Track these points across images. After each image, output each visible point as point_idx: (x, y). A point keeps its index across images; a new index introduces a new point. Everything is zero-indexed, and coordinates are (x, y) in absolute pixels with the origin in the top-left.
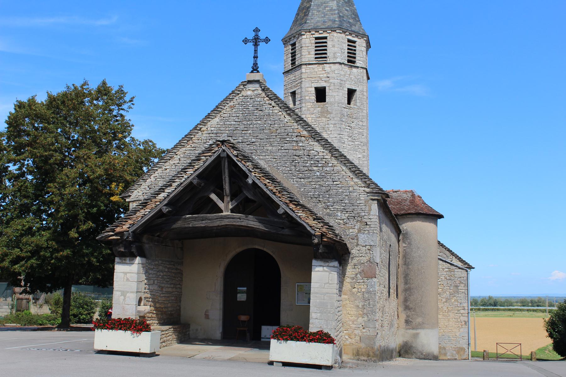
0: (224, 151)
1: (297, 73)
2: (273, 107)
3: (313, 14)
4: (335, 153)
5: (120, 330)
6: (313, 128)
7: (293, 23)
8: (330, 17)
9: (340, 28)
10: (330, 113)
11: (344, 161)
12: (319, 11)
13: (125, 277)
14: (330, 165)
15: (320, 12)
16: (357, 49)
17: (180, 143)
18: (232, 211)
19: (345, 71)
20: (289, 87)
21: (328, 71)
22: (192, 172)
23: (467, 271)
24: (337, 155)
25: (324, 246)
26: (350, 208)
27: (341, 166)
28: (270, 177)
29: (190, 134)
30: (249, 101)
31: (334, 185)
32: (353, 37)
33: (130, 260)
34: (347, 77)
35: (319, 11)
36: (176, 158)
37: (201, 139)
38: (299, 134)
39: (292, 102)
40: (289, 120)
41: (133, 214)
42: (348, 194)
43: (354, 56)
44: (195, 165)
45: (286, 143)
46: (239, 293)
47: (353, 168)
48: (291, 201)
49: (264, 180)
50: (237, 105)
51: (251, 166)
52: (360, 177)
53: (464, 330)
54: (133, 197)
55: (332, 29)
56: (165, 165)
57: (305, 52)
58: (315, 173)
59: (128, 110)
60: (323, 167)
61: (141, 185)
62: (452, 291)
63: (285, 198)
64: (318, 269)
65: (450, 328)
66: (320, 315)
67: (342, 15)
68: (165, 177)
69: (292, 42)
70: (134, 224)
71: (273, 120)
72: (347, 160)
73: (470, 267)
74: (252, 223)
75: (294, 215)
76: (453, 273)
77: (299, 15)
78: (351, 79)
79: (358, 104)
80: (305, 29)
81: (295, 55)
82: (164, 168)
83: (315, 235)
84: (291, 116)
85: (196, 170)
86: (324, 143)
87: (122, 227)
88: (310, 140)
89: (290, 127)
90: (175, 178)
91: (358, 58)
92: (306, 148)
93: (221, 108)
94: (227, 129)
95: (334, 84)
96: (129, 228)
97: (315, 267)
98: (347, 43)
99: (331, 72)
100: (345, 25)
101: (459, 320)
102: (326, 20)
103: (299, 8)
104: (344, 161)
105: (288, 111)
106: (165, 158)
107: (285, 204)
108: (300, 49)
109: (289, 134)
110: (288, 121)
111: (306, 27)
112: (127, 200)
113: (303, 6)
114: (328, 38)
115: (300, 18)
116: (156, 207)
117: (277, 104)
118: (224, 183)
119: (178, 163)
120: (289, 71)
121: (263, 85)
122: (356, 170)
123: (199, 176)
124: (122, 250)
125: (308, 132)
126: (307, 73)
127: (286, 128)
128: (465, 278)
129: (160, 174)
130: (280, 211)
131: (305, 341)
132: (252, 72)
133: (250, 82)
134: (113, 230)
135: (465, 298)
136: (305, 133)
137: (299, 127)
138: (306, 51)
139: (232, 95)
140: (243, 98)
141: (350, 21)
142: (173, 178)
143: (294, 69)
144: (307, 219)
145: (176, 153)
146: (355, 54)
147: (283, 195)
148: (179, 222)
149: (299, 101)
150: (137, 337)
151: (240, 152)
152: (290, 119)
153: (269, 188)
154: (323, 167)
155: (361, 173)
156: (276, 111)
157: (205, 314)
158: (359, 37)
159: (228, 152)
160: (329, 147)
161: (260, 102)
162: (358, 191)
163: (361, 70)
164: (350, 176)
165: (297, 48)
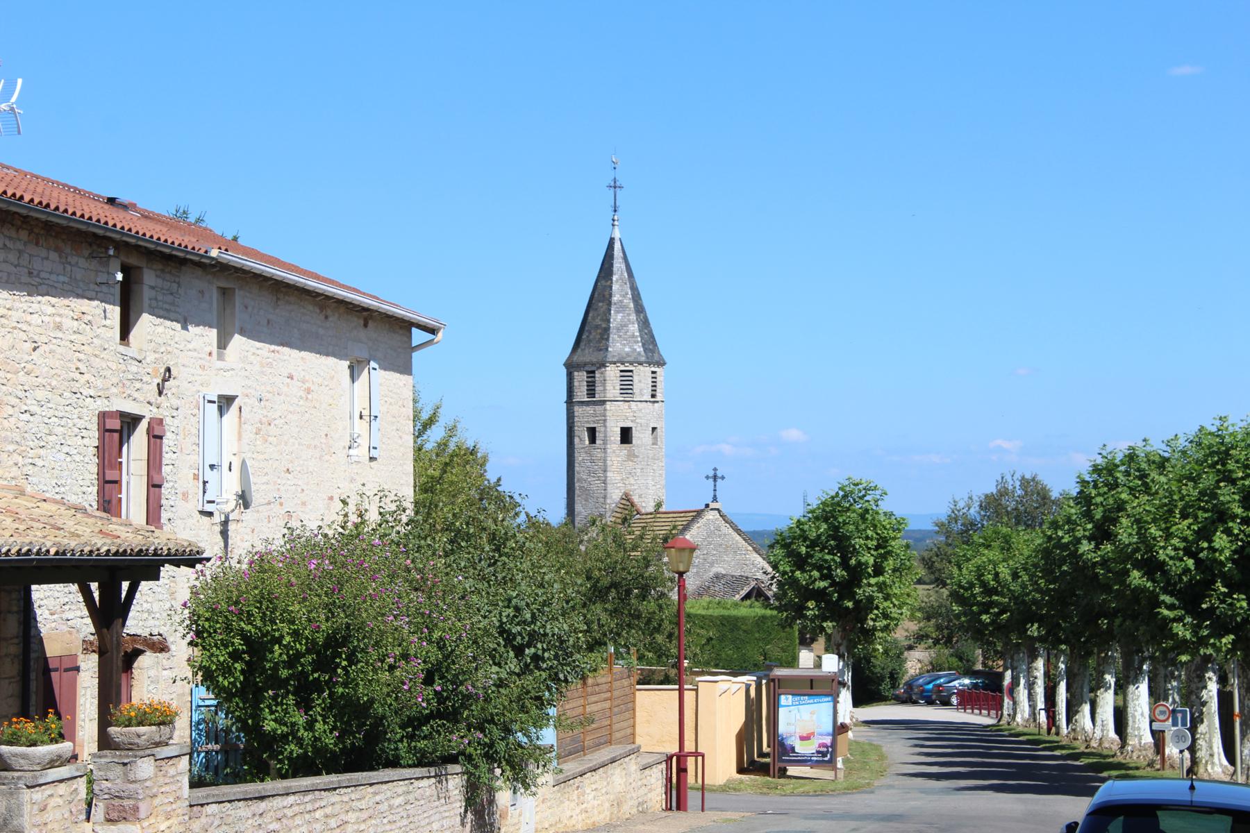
9: (646, 362)
10: (637, 457)
57: (609, 386)
79: (659, 443)
136: (750, 548)
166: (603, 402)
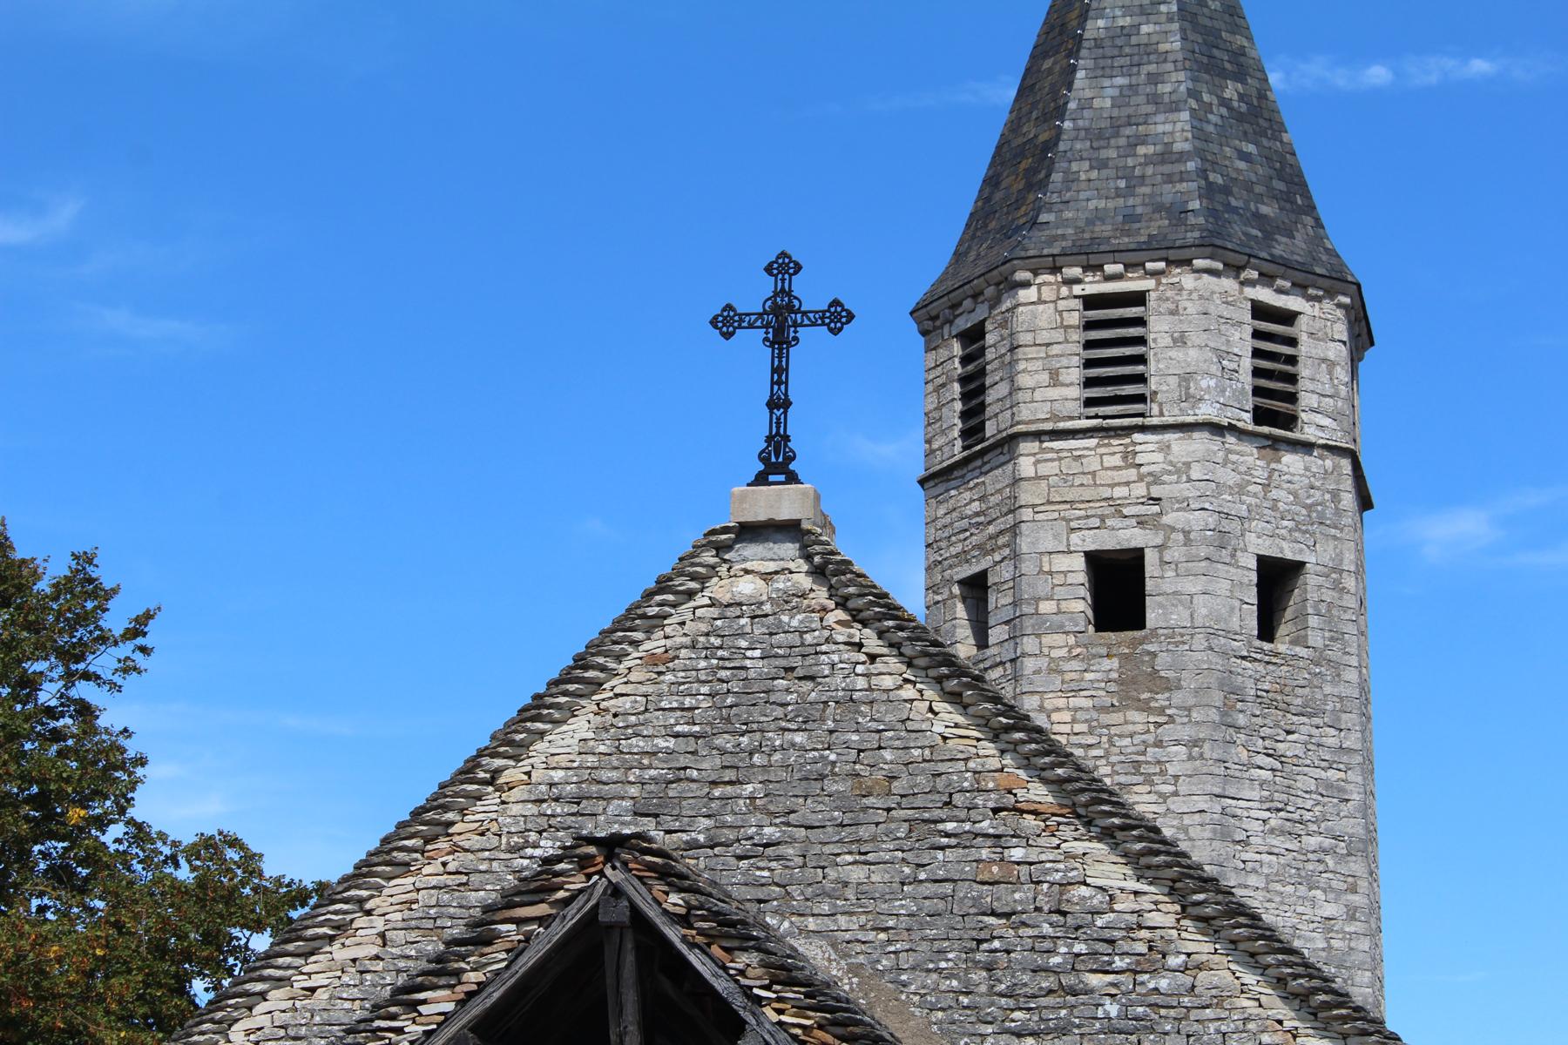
0: (616, 891)
1: (995, 480)
2: (873, 658)
3: (1071, 180)
6: (1079, 768)
7: (968, 226)
8: (1157, 190)
10: (1169, 686)
11: (1249, 939)
12: (1103, 165)
14: (1174, 961)
19: (1243, 469)
20: (953, 550)
24: (1208, 910)
28: (857, 1030)
29: (438, 802)
32: (1280, 291)
34: (1255, 495)
35: (1103, 165)
37: (494, 828)
39: (969, 632)
40: (957, 726)
43: (1289, 388)
44: (465, 971)
45: (942, 848)
47: (1296, 977)
50: (683, 653)
51: (760, 971)
52: (1336, 1025)
55: (1172, 254)
56: (305, 969)
57: (1031, 375)
58: (1098, 1005)
59: (117, 679)
60: (1136, 972)
67: (1220, 181)
68: (303, 1031)
69: (964, 323)
71: (873, 725)
78: (1274, 508)
79: (1315, 639)
80: (1031, 253)
81: (982, 389)
82: (301, 982)
84: (965, 707)
85: (470, 995)
86: (1139, 846)
88: (1067, 832)
89: (960, 766)
91: (1307, 399)
92: (1047, 872)
93: (603, 669)
94: (632, 778)
95: (1186, 533)
99: (1169, 473)
102: (1139, 210)
103: (999, 148)
104: (1249, 939)
105: (948, 677)
106: (310, 932)
108: (1007, 358)
109: (958, 799)
110: (948, 732)
111: (1034, 243)
113: (1020, 140)
117: (891, 645)
119: (377, 957)
122: (1315, 991)
126: (1046, 478)
127: (942, 767)
129: (280, 1019)
132: (761, 480)
133: (750, 532)
136: (1038, 793)
137: (1008, 760)
138: (1038, 365)
139: (658, 598)
140: (714, 612)
141: (1264, 209)
143: (978, 463)
145: (368, 906)
146: (1292, 379)
149: (1006, 623)
151: (703, 898)
152: (960, 719)
155: (1340, 1005)
156: (888, 682)
158: (1311, 291)
160: (1169, 866)
161: (802, 633)
163: (1328, 463)
164: (1280, 1022)
165: (990, 354)
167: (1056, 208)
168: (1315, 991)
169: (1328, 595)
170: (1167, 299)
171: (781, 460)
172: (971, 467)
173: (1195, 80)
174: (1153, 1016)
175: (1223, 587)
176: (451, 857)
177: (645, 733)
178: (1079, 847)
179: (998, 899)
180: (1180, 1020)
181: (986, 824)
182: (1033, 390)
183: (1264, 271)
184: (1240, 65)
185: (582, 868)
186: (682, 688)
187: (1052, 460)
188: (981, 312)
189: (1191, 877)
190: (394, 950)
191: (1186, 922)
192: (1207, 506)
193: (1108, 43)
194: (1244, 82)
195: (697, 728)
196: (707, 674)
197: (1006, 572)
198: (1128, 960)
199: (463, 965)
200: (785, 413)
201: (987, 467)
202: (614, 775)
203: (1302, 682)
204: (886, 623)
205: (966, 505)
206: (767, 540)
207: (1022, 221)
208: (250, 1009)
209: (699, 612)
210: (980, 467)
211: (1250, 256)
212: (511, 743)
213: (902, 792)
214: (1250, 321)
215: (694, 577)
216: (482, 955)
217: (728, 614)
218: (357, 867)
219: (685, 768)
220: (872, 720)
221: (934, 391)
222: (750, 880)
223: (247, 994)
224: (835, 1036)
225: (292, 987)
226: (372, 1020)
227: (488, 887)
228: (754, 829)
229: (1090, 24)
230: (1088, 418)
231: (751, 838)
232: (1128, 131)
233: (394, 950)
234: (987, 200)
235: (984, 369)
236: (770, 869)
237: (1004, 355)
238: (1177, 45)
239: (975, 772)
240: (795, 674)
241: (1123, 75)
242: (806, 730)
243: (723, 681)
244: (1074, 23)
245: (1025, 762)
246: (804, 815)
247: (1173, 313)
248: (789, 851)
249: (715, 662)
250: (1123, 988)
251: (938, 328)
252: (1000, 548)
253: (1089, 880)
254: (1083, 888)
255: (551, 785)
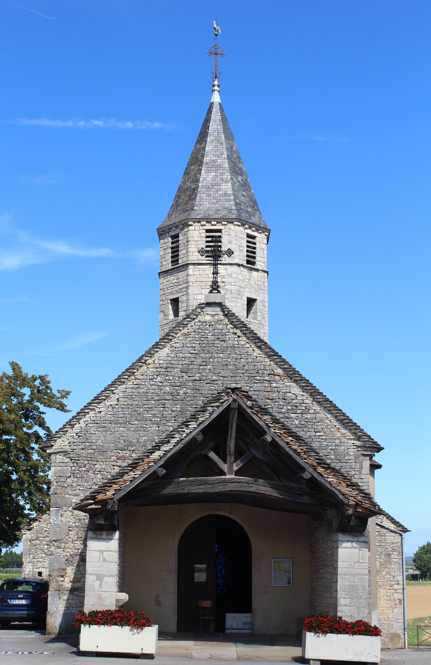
0: (234, 400)
1: (181, 275)
3: (201, 199)
4: (319, 397)
5: (114, 625)
6: (290, 365)
9: (239, 220)
11: (330, 407)
12: (210, 195)
13: (101, 557)
14: (311, 411)
15: (211, 196)
16: (257, 246)
17: (120, 379)
18: (237, 473)
21: (222, 274)
22: (196, 426)
23: (401, 535)
24: (320, 400)
25: (356, 517)
26: (337, 465)
27: (325, 413)
28: (294, 434)
29: (132, 367)
30: (208, 328)
31: (317, 437)
32: (253, 231)
33: (107, 535)
35: (210, 195)
36: (114, 397)
37: (146, 374)
38: (272, 372)
40: (259, 354)
41: (120, 477)
42: (335, 447)
44: (199, 418)
45: (256, 383)
46: (197, 572)
47: (340, 416)
48: (319, 464)
49: (286, 437)
51: (270, 420)
52: (349, 427)
53: (398, 610)
54: (56, 448)
55: (229, 221)
56: (98, 407)
58: (293, 421)
60: (302, 414)
61: (67, 431)
62: (382, 560)
63: (312, 460)
64: (345, 545)
65: (380, 608)
66: (350, 601)
67: (239, 202)
68: (99, 422)
69: (173, 233)
70: (121, 490)
71: (239, 353)
72: (333, 407)
73: (405, 530)
74: (263, 488)
75: (322, 481)
76: (384, 537)
77: (180, 198)
79: (259, 318)
80: (193, 217)
81: (178, 251)
82: (97, 410)
83: (348, 505)
84: (261, 350)
85: (200, 423)
86: (304, 384)
87: (105, 493)
88: (286, 380)
89: (260, 363)
90: (175, 433)
91: (258, 258)
92: (281, 390)
93: (173, 336)
95: (231, 291)
96: (114, 494)
97: (342, 542)
98: (246, 239)
100: (244, 216)
101: (392, 598)
102: (219, 208)
103: (179, 188)
104: (330, 407)
105: (258, 342)
106: (101, 398)
107: (312, 467)
108: (186, 244)
109: (260, 371)
110: (257, 355)
111: (194, 215)
112: (48, 451)
113: (186, 187)
114: (223, 231)
115: (183, 201)
116: (148, 468)
117: (243, 334)
118: (229, 438)
119: (117, 404)
120: (168, 270)
121: (227, 310)
122: (345, 419)
123: (204, 431)
124: (101, 522)
125: (283, 370)
128: (399, 544)
129: (92, 419)
130: (307, 476)
131: (347, 633)
133: (208, 304)
134: (93, 498)
135: (400, 570)
136: (279, 371)
137: (272, 363)
138: (194, 246)
139: (187, 320)
140: (200, 324)
141: (249, 210)
142: (173, 433)
143: (177, 270)
144: (339, 485)
145: (114, 392)
146: (254, 253)
147: (309, 456)
148: (171, 486)
149: (184, 311)
150: (138, 633)
151: (257, 403)
152: (260, 353)
153: (293, 447)
154: (302, 414)
156: (243, 343)
157: (156, 600)
158: (260, 231)
159: (241, 403)
160: (311, 389)
161: (221, 330)
162: (346, 445)
163: (262, 274)
164: (335, 426)
165: (180, 242)
166: (186, 266)
167: (198, 206)
168: (345, 419)
169: (262, 307)
170: (227, 232)
171: (216, 287)
172: (174, 271)
173: (232, 175)
174: (306, 424)
175: (239, 305)
176: (135, 381)
177: (183, 352)
178: (289, 384)
179: (270, 396)
180: (312, 425)
181: (267, 378)
182: (193, 252)
183: (250, 226)
184: (241, 172)
185: (227, 395)
186: (192, 342)
187: (197, 271)
188: (177, 231)
189: (317, 392)
190: (121, 403)
191: (314, 402)
192: (236, 284)
193: (209, 164)
194: (243, 176)
195: (196, 352)
196: (198, 339)
197: (185, 298)
198: (300, 411)
199: (199, 416)
200: (217, 276)
201: (179, 271)
202: (176, 362)
203: (256, 329)
204: (243, 329)
205: (172, 280)
206: (213, 307)
207: (189, 208)
208: (85, 416)
209: (196, 323)
210: (177, 271)
211: (247, 222)
212: (150, 354)
213: (247, 369)
214: (246, 238)
215: (195, 315)
216: (203, 414)
217: (203, 324)
218: (112, 382)
219: (193, 361)
220: (239, 352)
221: (163, 250)
222: (210, 389)
223: (85, 412)
224: (288, 435)
225: (95, 411)
226: (178, 429)
227: (144, 388)
228: (210, 377)
229: (205, 158)
230: (206, 260)
231: (210, 379)
232: (216, 187)
233: (121, 403)
234: (177, 201)
235: (178, 246)
236: (214, 387)
237: (185, 243)
238: (227, 166)
239: (264, 365)
240: (220, 340)
241: (214, 172)
242: (223, 353)
243: (202, 341)
244: (200, 157)
245: (276, 363)
246: (223, 374)
247: (228, 235)
248: (219, 382)
249: (200, 336)
250: (299, 417)
251: (165, 234)
252: (183, 292)
253: (291, 392)
254: (290, 393)
255: (160, 364)
